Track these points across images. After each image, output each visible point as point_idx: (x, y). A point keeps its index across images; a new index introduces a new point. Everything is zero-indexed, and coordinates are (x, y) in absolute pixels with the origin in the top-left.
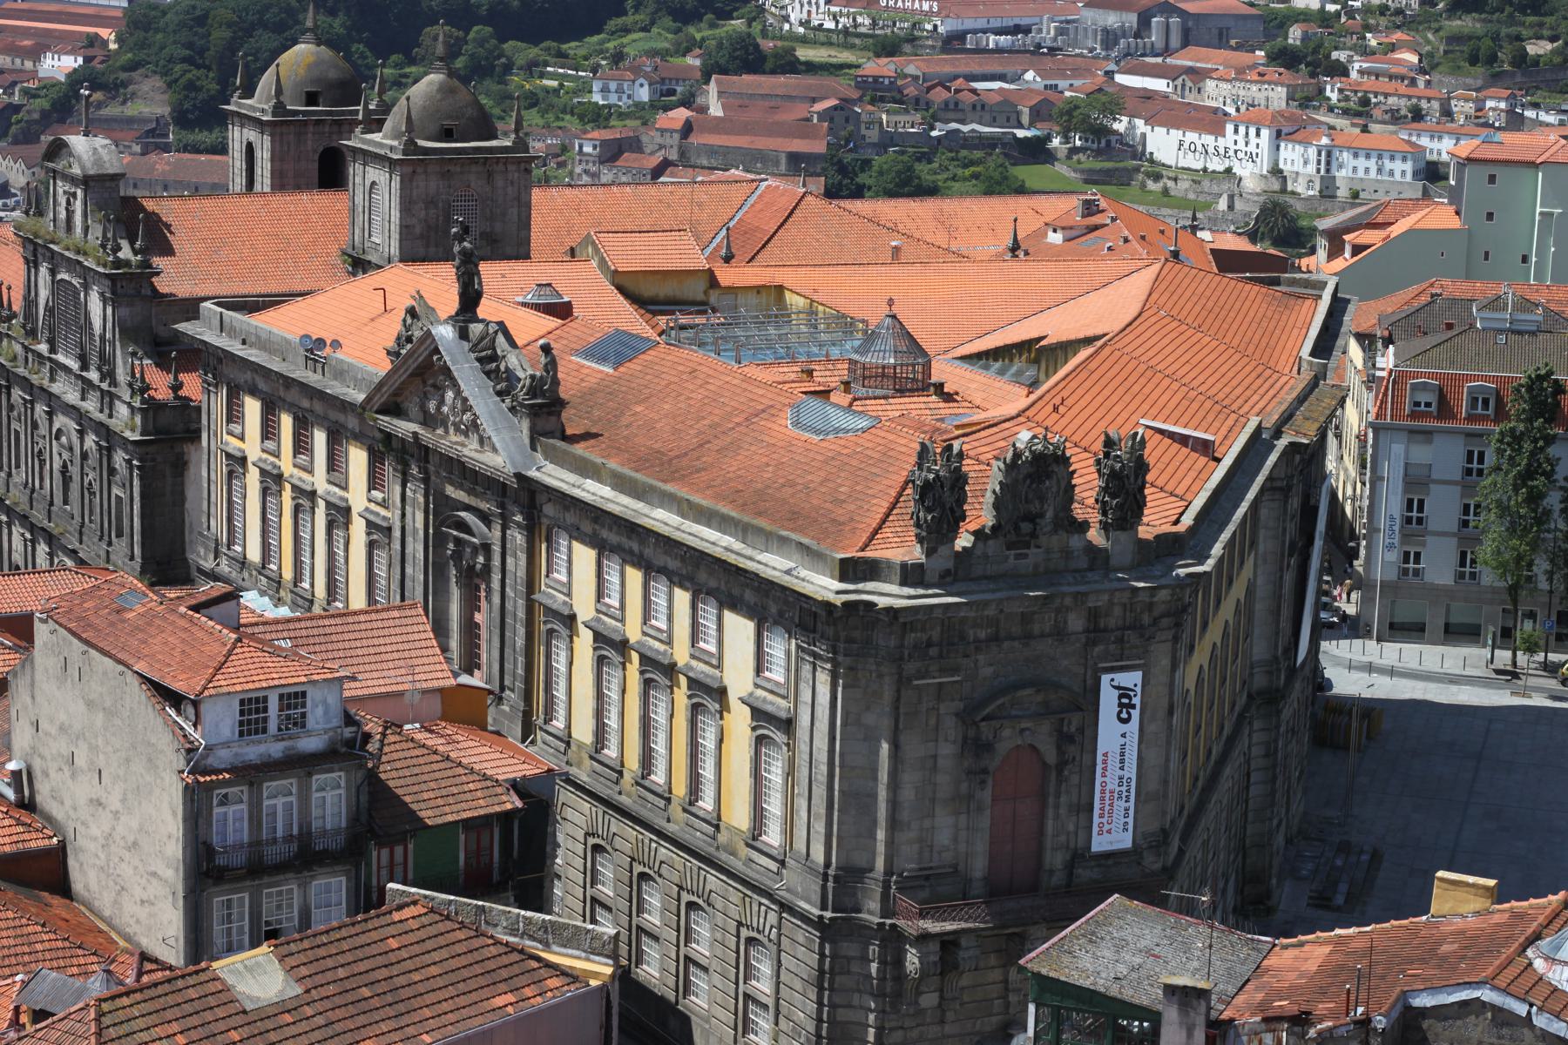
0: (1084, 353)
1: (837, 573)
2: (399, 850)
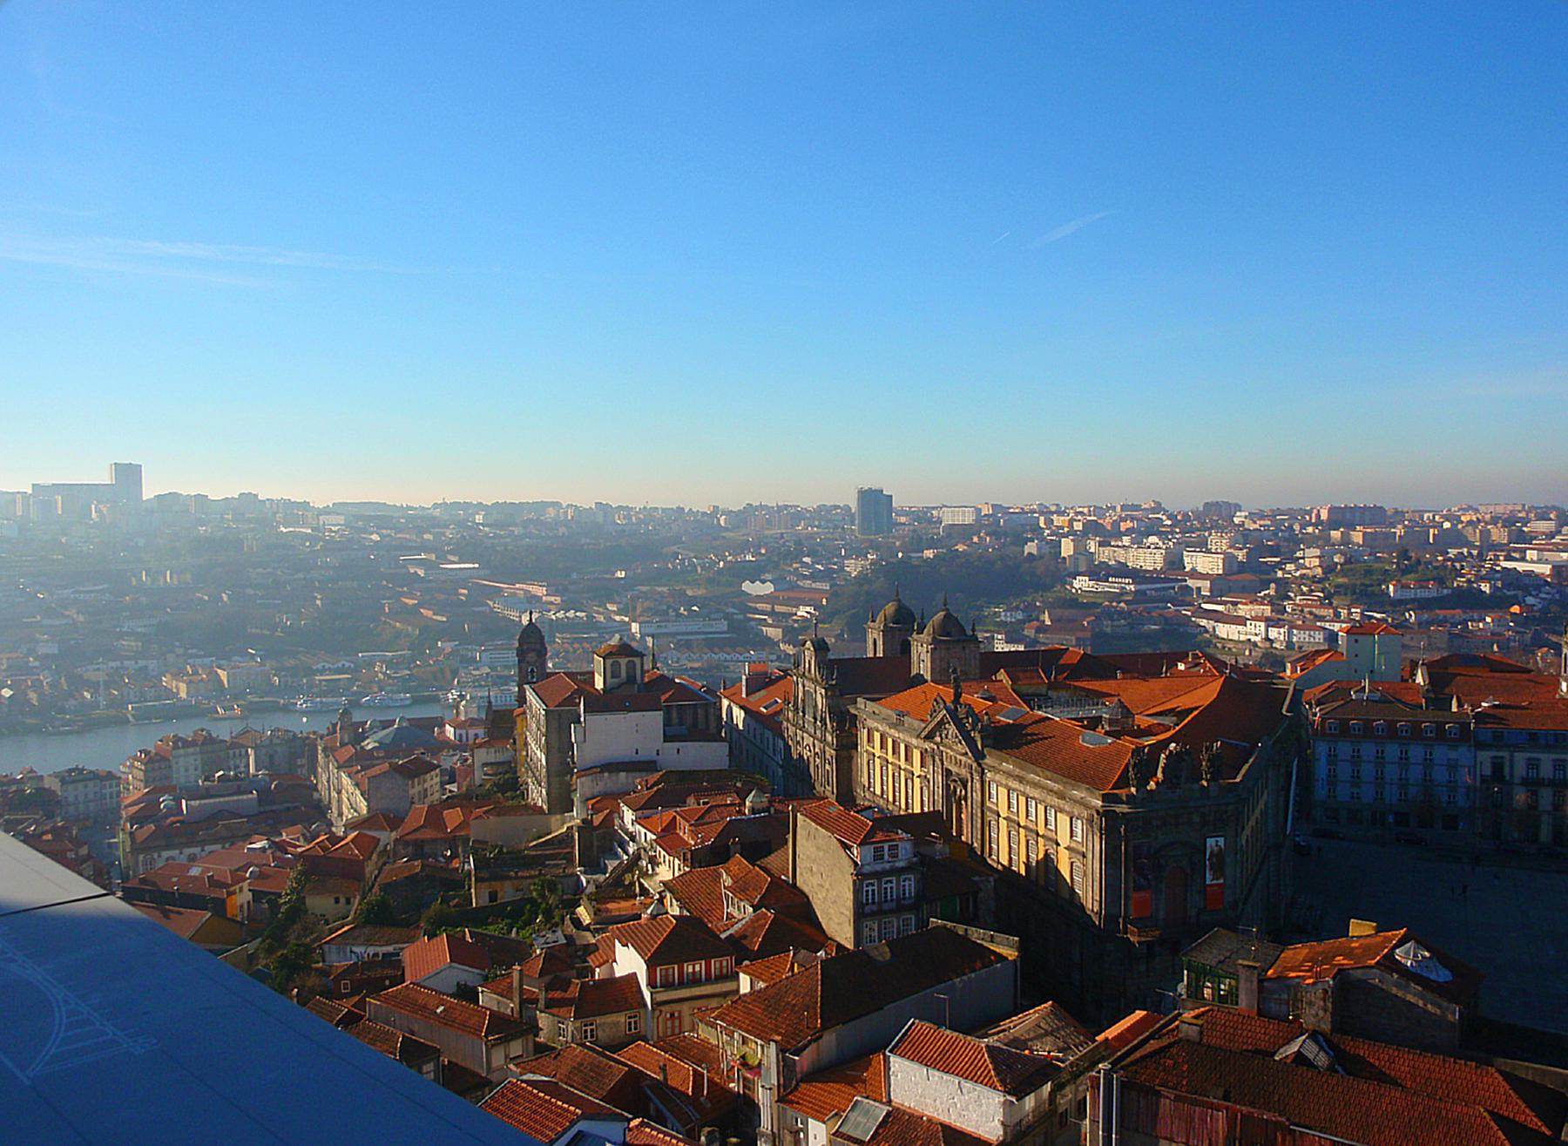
0: (1196, 713)
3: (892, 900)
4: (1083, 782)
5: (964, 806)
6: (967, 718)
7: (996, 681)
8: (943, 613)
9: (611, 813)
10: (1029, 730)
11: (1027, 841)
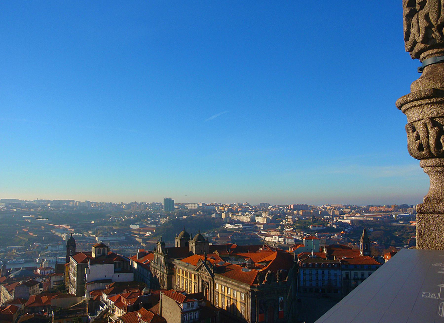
3: (192, 320)
4: (244, 282)
5: (208, 291)
6: (209, 264)
7: (214, 254)
8: (198, 234)
9: (99, 296)
10: (226, 268)
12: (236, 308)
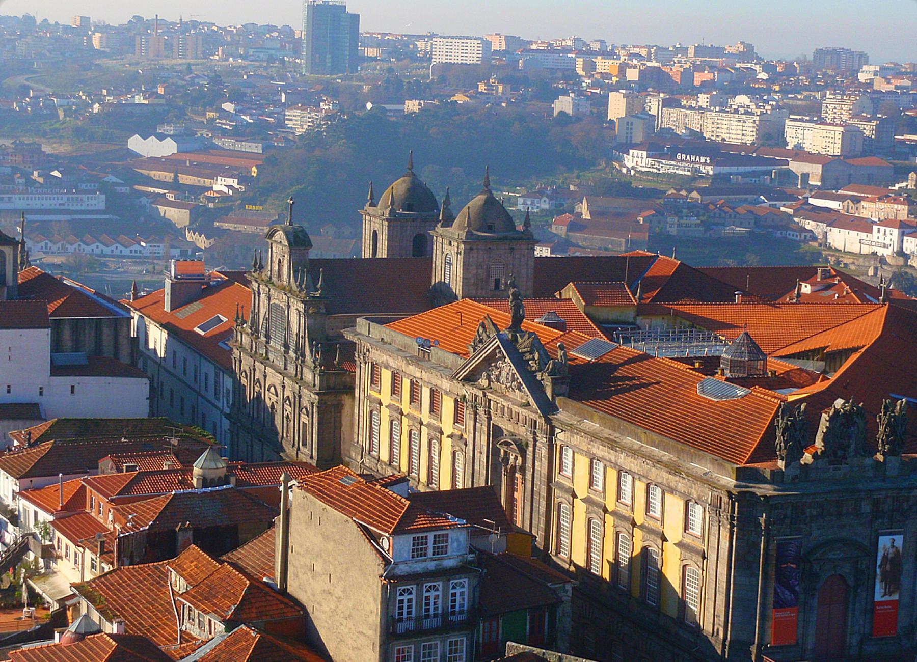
0: (854, 357)
1: (734, 476)
2: (494, 624)
3: (436, 615)
6: (531, 352)
7: (561, 300)
10: (620, 373)
11: (617, 534)
12: (660, 571)
